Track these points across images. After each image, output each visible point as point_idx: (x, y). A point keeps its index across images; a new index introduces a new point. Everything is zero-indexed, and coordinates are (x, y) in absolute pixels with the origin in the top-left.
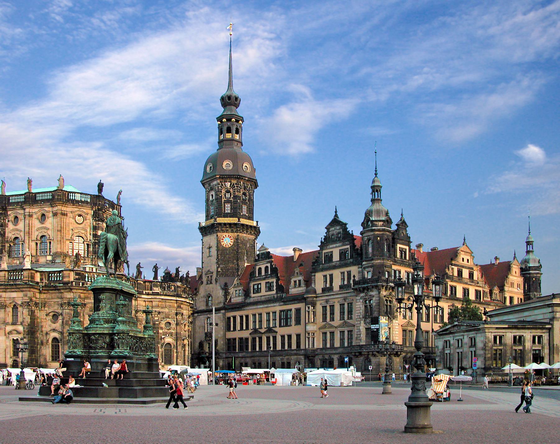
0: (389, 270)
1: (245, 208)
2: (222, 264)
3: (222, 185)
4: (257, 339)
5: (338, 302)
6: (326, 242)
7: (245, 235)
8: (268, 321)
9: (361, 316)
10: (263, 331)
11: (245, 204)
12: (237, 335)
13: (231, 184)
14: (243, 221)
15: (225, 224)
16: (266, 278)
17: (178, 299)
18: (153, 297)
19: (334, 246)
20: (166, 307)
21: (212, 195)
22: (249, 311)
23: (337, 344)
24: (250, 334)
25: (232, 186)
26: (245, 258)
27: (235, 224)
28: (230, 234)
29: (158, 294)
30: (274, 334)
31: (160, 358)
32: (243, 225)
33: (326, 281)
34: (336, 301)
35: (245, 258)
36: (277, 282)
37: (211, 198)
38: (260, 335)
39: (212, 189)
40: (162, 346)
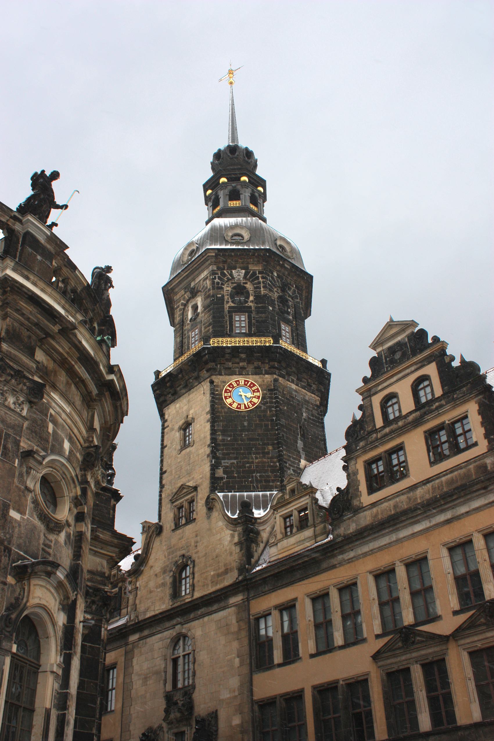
3: (224, 275)
7: (294, 386)
11: (288, 322)
12: (306, 675)
15: (235, 350)
22: (360, 567)
24: (376, 657)
25: (251, 277)
26: (300, 444)
27: (265, 350)
28: (251, 379)
37: (190, 315)
38: (430, 651)
39: (194, 293)
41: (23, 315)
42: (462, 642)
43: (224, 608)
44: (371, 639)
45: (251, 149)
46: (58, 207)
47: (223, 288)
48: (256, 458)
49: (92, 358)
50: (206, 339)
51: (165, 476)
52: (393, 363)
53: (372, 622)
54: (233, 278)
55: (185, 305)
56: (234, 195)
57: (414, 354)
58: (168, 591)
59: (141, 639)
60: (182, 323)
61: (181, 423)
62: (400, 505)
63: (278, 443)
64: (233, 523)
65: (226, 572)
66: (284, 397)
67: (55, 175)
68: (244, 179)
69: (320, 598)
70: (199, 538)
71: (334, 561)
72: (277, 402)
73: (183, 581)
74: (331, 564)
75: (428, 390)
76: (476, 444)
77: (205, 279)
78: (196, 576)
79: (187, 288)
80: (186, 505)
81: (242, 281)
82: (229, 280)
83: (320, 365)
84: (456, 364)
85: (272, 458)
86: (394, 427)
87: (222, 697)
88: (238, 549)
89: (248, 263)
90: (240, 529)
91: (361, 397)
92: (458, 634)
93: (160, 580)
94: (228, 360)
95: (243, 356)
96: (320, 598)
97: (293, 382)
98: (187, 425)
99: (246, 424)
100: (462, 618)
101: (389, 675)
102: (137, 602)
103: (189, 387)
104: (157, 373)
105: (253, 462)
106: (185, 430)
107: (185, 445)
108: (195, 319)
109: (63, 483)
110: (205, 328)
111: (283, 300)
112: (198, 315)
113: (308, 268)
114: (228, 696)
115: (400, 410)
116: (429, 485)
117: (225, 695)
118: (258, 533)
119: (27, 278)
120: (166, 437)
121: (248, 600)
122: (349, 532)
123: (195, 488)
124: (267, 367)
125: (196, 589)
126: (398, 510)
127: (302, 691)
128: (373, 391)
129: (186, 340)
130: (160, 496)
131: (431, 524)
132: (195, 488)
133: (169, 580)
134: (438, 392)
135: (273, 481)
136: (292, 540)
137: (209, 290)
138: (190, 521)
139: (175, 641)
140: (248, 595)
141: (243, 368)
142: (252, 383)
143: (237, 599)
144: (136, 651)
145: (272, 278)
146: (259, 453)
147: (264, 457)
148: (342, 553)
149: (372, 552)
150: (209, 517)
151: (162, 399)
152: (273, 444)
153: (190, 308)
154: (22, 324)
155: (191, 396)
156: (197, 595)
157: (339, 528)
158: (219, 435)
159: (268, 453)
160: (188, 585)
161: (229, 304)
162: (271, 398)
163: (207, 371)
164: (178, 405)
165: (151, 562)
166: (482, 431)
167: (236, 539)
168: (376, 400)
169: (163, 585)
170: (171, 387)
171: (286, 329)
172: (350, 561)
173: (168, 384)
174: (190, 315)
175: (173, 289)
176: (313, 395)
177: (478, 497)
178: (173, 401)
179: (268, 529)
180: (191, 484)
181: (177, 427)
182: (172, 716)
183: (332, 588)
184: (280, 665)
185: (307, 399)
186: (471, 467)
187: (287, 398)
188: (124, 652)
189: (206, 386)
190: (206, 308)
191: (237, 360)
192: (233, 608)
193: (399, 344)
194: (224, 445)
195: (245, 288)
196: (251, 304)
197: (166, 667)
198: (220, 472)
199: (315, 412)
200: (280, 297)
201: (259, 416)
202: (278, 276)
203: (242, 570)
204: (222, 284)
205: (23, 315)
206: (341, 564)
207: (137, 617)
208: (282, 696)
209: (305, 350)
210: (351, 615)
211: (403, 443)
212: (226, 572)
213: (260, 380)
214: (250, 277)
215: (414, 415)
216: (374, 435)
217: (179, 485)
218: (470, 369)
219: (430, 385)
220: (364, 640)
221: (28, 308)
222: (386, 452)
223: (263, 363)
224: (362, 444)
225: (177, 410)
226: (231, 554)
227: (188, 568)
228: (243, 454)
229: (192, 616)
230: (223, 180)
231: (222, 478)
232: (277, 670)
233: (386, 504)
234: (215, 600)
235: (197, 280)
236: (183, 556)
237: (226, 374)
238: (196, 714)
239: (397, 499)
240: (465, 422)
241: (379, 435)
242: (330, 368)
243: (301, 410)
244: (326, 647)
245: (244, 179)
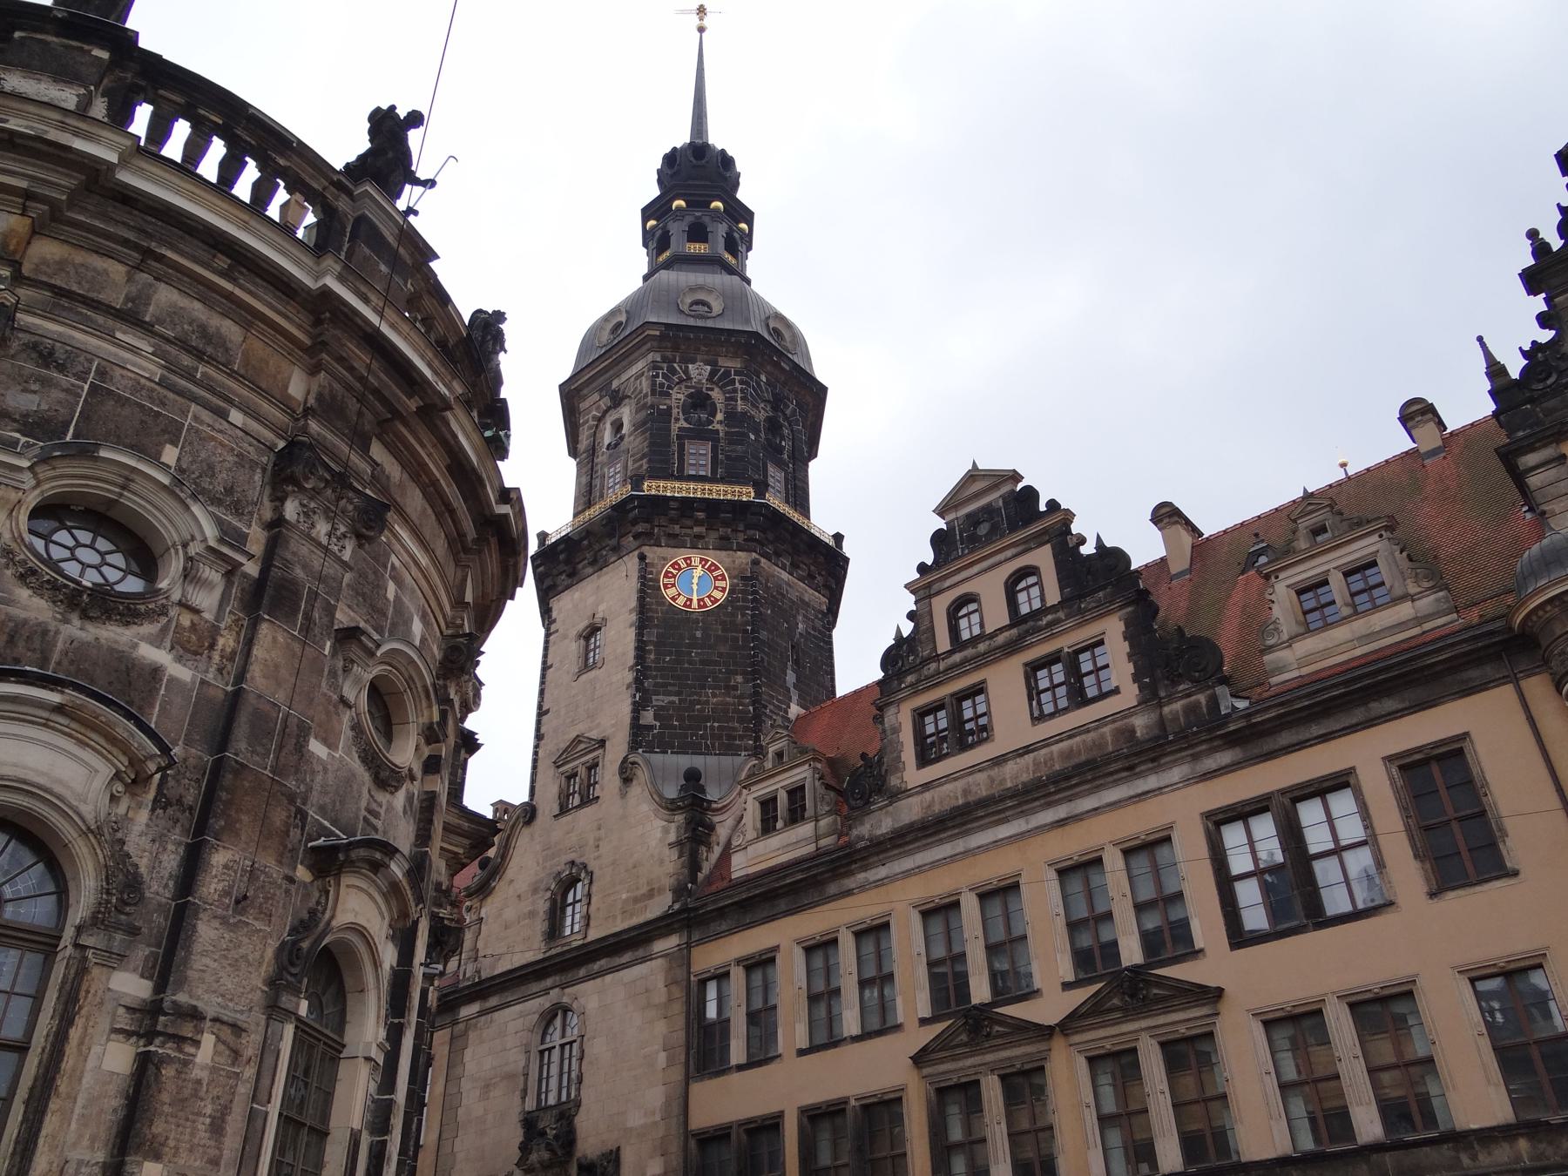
2: (662, 689)
3: (674, 372)
7: (785, 576)
11: (780, 464)
12: (787, 1087)
13: (713, 374)
15: (687, 504)
20: (131, 317)
21: (618, 426)
22: (895, 895)
24: (920, 1059)
25: (721, 378)
26: (791, 677)
27: (739, 509)
30: (1181, 1020)
35: (791, 677)
38: (1018, 1053)
39: (617, 399)
41: (351, 369)
42: (1077, 1038)
43: (644, 960)
44: (911, 1025)
45: (730, 153)
46: (417, 182)
47: (669, 395)
48: (714, 695)
49: (474, 469)
50: (637, 482)
51: (545, 718)
52: (974, 542)
53: (913, 996)
54: (689, 378)
55: (600, 420)
56: (698, 233)
57: (1013, 528)
58: (540, 926)
59: (482, 1013)
60: (592, 451)
61: (583, 625)
62: (974, 789)
63: (754, 672)
64: (671, 807)
65: (651, 894)
67: (416, 119)
68: (718, 204)
69: (820, 948)
70: (602, 831)
71: (850, 883)
72: (753, 601)
73: (569, 909)
74: (845, 888)
75: (1035, 591)
76: (1116, 691)
77: (639, 376)
78: (594, 900)
79: (605, 389)
80: (582, 771)
81: (706, 385)
82: (681, 381)
83: (832, 543)
84: (1088, 549)
85: (741, 697)
86: (969, 652)
87: (630, 1124)
88: (674, 854)
90: (680, 818)
91: (913, 598)
92: (1070, 1024)
93: (526, 907)
94: (673, 521)
95: (701, 515)
96: (820, 948)
98: (593, 630)
99: (699, 634)
100: (1081, 995)
101: (941, 1092)
102: (480, 945)
103: (599, 564)
105: (707, 702)
106: (587, 639)
108: (616, 445)
109: (408, 698)
110: (635, 462)
111: (773, 426)
112: (622, 438)
113: (821, 373)
114: (642, 1121)
115: (982, 625)
116: (1029, 758)
117: (636, 1120)
118: (711, 828)
119: (366, 300)
120: (551, 650)
121: (689, 946)
122: (879, 832)
123: (602, 743)
124: (741, 537)
125: (592, 923)
126: (971, 799)
127: (781, 1115)
128: (936, 587)
129: (597, 482)
130: (536, 753)
131: (1030, 826)
132: (602, 743)
133: (542, 906)
134: (1054, 597)
135: (741, 738)
136: (774, 842)
137: (646, 396)
138: (588, 800)
139: (548, 1018)
140: (689, 937)
141: (699, 537)
144: (472, 1035)
145: (758, 384)
148: (865, 869)
149: (919, 870)
150: (623, 795)
151: (548, 582)
152: (744, 673)
153: (608, 426)
154: (349, 388)
155: (604, 579)
156: (593, 935)
157: (862, 824)
158: (650, 652)
159: (735, 688)
160: (577, 917)
161: (679, 424)
162: (744, 592)
163: (636, 537)
164: (577, 595)
165: (511, 871)
166: (1130, 668)
167: (672, 837)
168: (940, 605)
169: (532, 914)
170: (567, 562)
171: (775, 476)
172: (879, 883)
173: (562, 557)
174: (607, 437)
175: (578, 390)
177: (1116, 783)
178: (568, 587)
179: (730, 822)
180: (594, 734)
181: (573, 633)
182: (534, 1157)
183: (843, 930)
184: (740, 1068)
186: (1107, 730)
188: (447, 1038)
189: (631, 564)
190: (638, 426)
191: (689, 522)
192: (660, 961)
193: (988, 510)
194: (657, 669)
195: (709, 397)
196: (718, 427)
197: (527, 1066)
198: (648, 717)
199: (818, 624)
200: (768, 419)
201: (723, 623)
202: (768, 383)
203: (679, 891)
204: (670, 387)
205: (351, 369)
206: (863, 888)
207: (478, 972)
208: (741, 1124)
209: (805, 512)
210: (878, 980)
211: (984, 682)
212: (651, 894)
213: (728, 560)
214: (720, 379)
215: (1007, 634)
216: (933, 666)
218: (1112, 558)
219: (1040, 583)
220: (898, 1028)
221: (361, 358)
222: (952, 695)
223: (735, 531)
224: (910, 679)
225: (575, 603)
226: (662, 862)
227: (579, 885)
229: (582, 972)
230: (680, 203)
231: (651, 727)
232: (736, 1077)
233: (948, 787)
235: (624, 377)
236: (573, 863)
237: (668, 546)
238: (578, 1154)
239: (970, 779)
240: (1097, 651)
241: (942, 666)
242: (847, 549)
243: (795, 617)
244: (825, 1040)
245: (718, 204)
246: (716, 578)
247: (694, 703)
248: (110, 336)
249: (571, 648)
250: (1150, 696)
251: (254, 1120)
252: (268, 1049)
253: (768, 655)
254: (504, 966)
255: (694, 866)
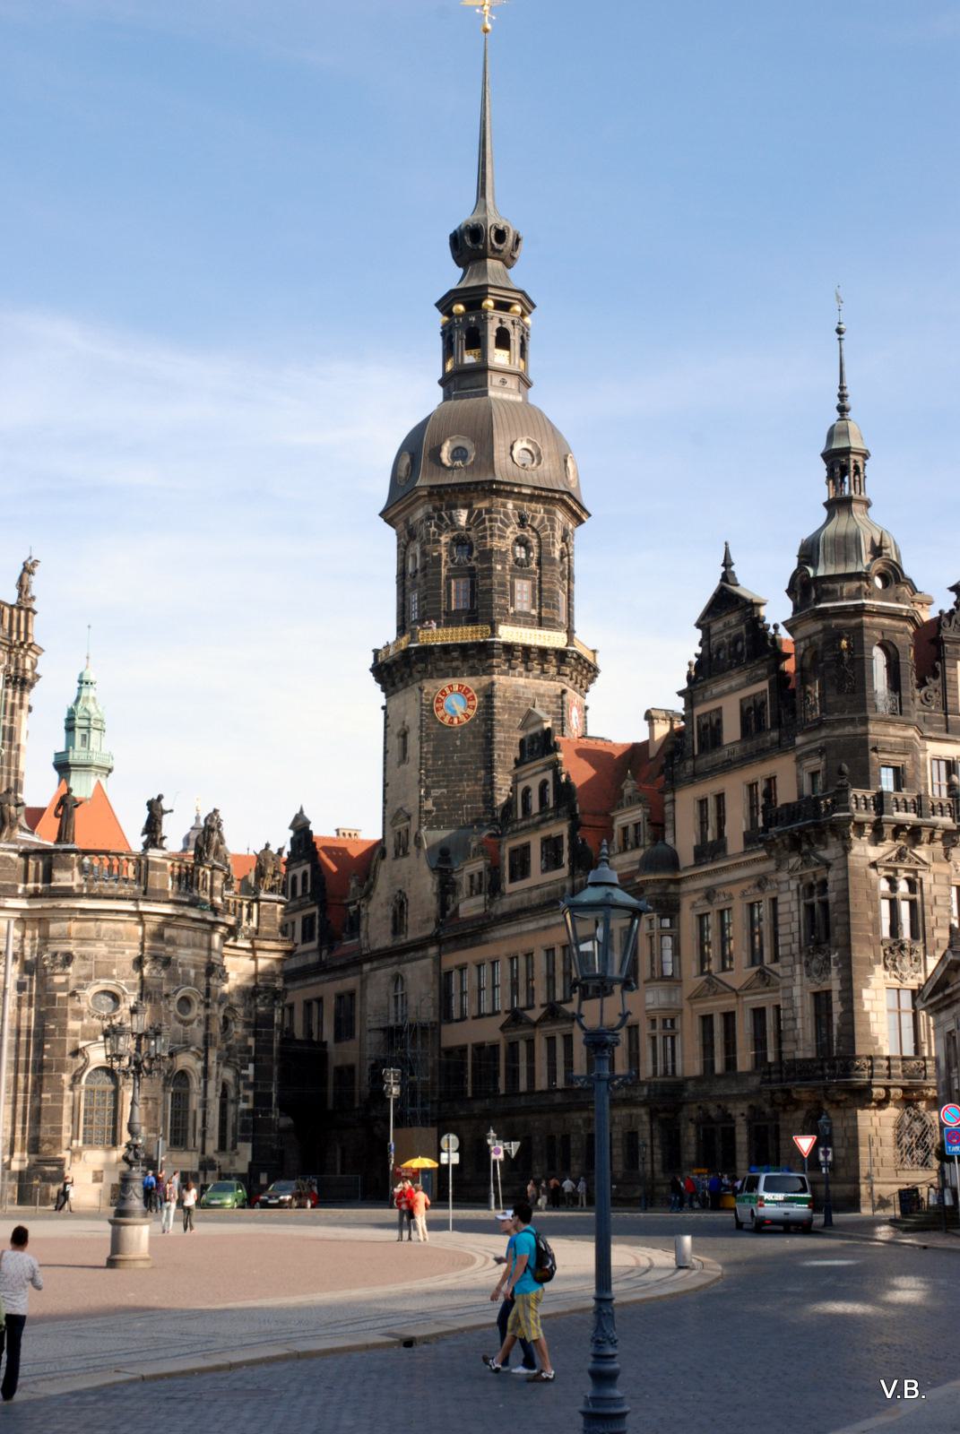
0: (899, 760)
1: (523, 589)
2: (436, 785)
3: (441, 518)
4: (522, 1047)
5: (743, 894)
6: (704, 673)
7: (522, 681)
8: (551, 978)
9: (795, 947)
10: (535, 1015)
14: (507, 633)
15: (446, 649)
16: (544, 821)
17: (143, 907)
18: (47, 904)
19: (725, 686)
20: (98, 939)
23: (745, 1061)
24: (502, 1028)
29: (67, 893)
30: (565, 1027)
31: (66, 1122)
32: (509, 648)
33: (703, 822)
34: (736, 890)
36: (572, 836)
40: (76, 1078)
43: (424, 957)
46: (167, 812)
48: (468, 786)
51: (387, 789)
66: (504, 702)
67: (160, 798)
88: (434, 900)
89: (472, 498)
95: (455, 654)
97: (521, 675)
99: (458, 743)
104: (376, 652)
105: (464, 791)
107: (404, 758)
120: (388, 739)
130: (384, 813)
132: (409, 818)
138: (406, 854)
141: (457, 668)
142: (467, 688)
143: (433, 951)
145: (506, 514)
146: (469, 780)
147: (474, 785)
164: (397, 702)
167: (435, 890)
169: (387, 917)
172: (496, 940)
176: (552, 683)
185: (542, 691)
187: (510, 702)
194: (433, 771)
198: (429, 805)
204: (440, 535)
211: (529, 842)
212: (428, 920)
213: (476, 684)
214: (474, 521)
217: (398, 806)
228: (454, 781)
231: (429, 812)
232: (455, 1025)
234: (419, 946)
246: (469, 699)
247: (455, 793)
248: (94, 946)
249: (395, 742)
250: (572, 874)
251: (165, 1116)
252: (165, 1101)
253: (504, 750)
254: (378, 946)
255: (444, 906)
